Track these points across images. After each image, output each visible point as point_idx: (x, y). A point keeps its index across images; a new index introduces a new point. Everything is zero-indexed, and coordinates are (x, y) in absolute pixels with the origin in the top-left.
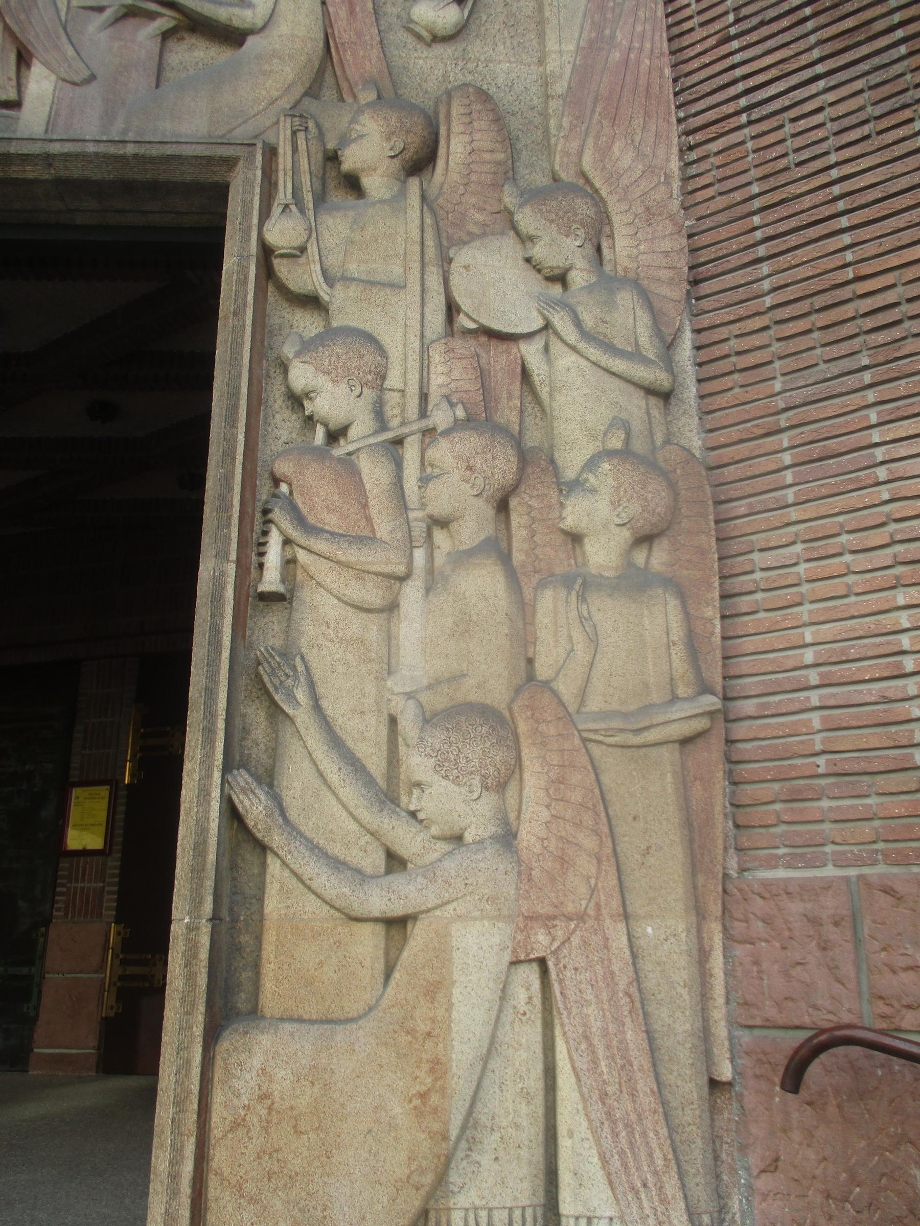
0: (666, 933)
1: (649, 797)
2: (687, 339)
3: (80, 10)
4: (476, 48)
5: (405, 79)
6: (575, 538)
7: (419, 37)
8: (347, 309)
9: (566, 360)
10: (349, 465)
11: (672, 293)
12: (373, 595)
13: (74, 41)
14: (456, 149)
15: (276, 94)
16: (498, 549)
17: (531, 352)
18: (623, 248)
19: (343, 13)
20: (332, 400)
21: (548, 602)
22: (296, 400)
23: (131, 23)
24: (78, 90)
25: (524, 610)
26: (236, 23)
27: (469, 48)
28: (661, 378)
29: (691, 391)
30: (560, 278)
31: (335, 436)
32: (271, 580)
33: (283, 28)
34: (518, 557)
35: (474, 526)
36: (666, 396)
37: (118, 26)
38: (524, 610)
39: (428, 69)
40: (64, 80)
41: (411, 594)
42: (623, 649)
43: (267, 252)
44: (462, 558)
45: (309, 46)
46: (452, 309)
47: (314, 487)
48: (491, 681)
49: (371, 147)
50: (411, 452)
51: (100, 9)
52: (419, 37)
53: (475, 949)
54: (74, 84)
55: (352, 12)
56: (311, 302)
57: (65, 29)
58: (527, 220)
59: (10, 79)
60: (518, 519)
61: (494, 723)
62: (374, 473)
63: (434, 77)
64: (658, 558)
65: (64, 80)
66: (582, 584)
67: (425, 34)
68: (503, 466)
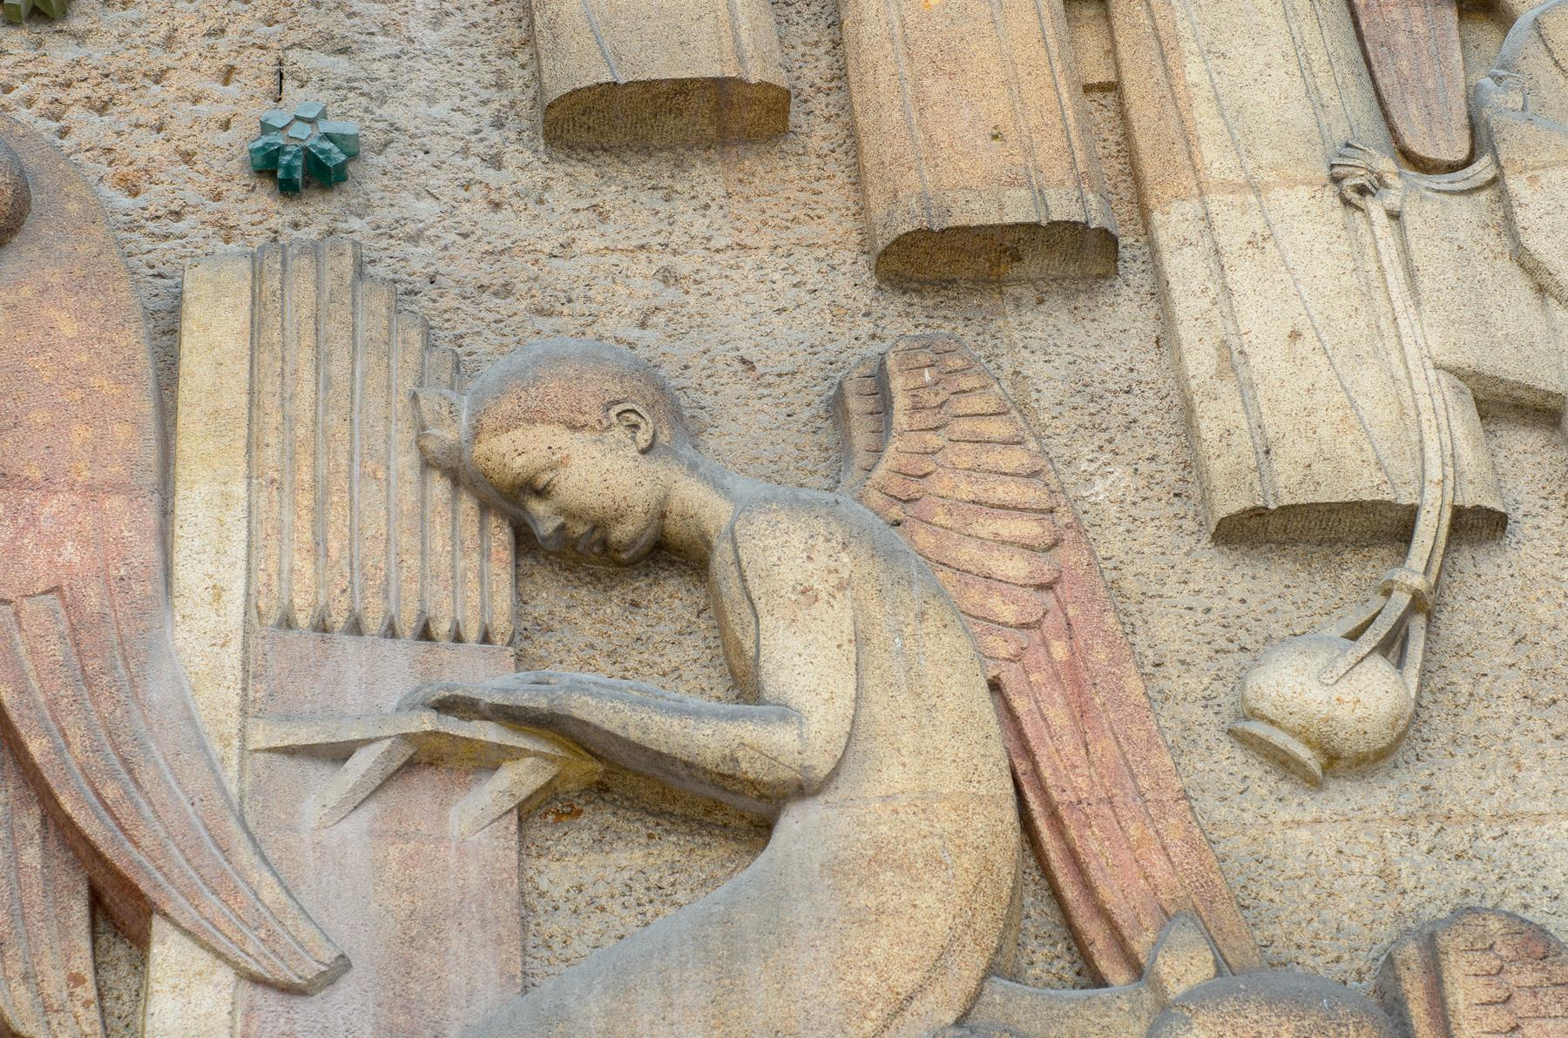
3: (280, 762)
4: (1460, 781)
5: (1267, 892)
7: (1283, 763)
13: (273, 856)
15: (907, 981)
19: (1058, 715)
23: (424, 787)
24: (303, 1008)
26: (751, 768)
27: (1440, 783)
33: (896, 775)
37: (392, 795)
40: (257, 980)
45: (978, 821)
51: (338, 754)
52: (1283, 763)
54: (288, 990)
55: (1082, 712)
57: (241, 820)
59: (77, 980)
63: (1354, 882)
65: (257, 980)
67: (1303, 753)
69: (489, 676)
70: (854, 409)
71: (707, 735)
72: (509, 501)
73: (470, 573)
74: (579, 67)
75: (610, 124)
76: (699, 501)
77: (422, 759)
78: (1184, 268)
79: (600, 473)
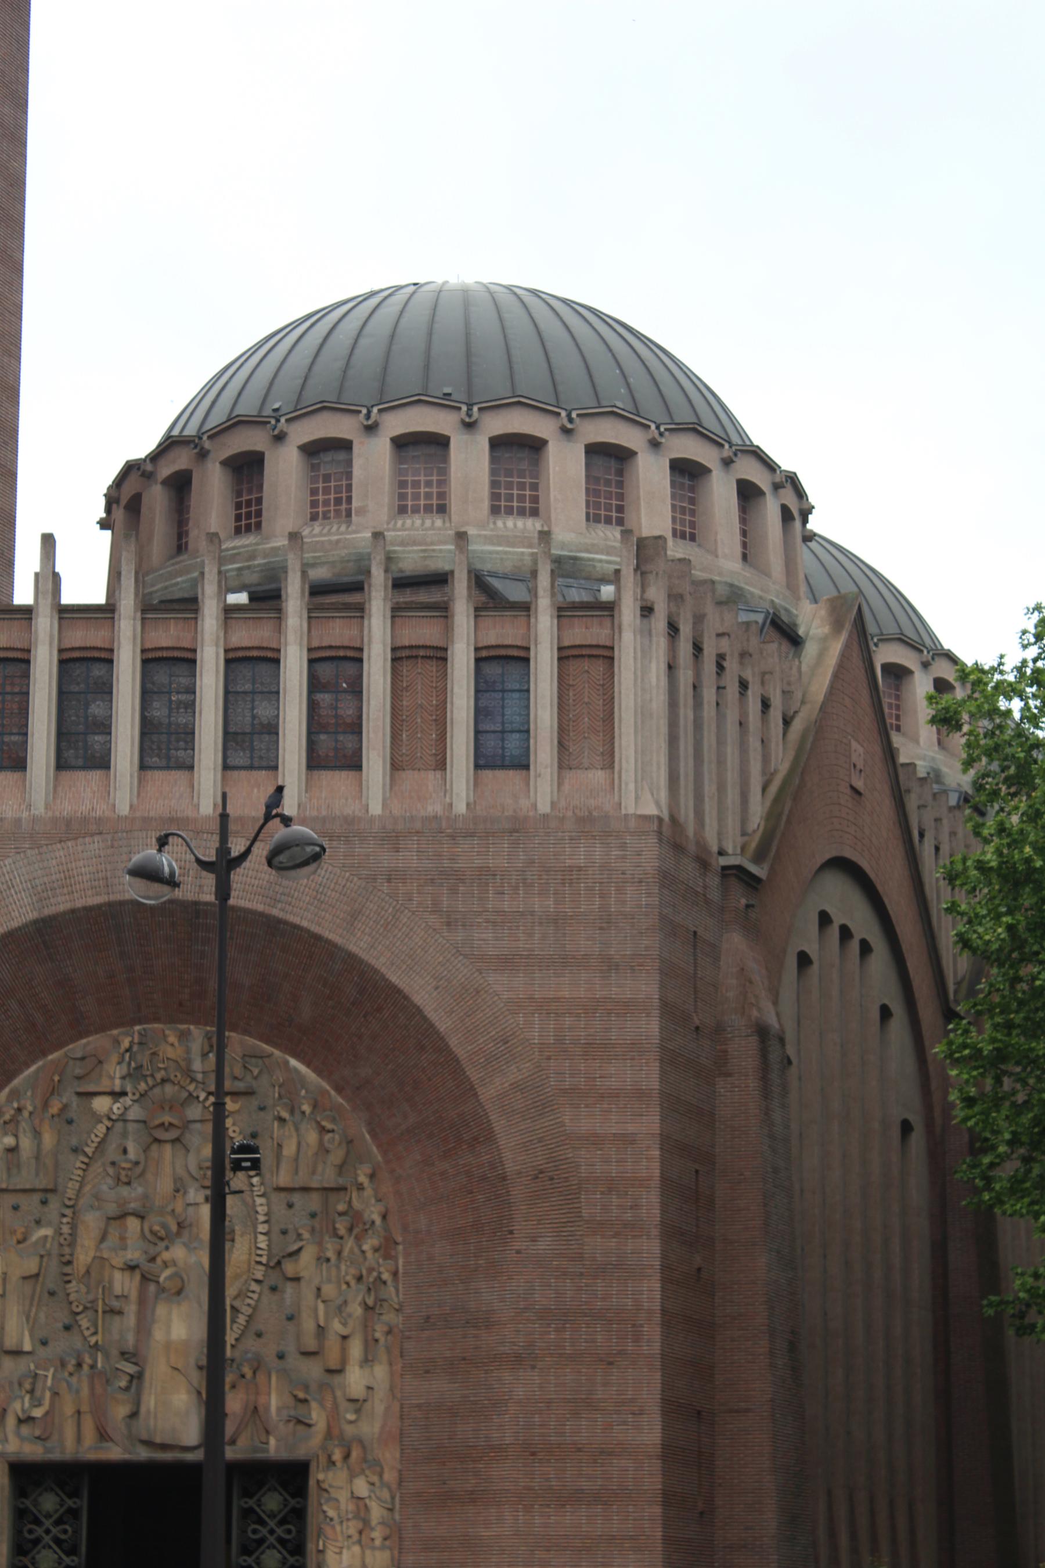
2: (398, 1495)
6: (373, 1539)
8: (334, 1493)
9: (374, 1503)
10: (333, 1527)
11: (394, 1486)
12: (337, 1550)
14: (354, 1454)
16: (359, 1542)
17: (367, 1501)
18: (387, 1476)
20: (331, 1513)
21: (368, 1552)
22: (324, 1512)
25: (363, 1552)
28: (390, 1506)
29: (397, 1506)
30: (373, 1484)
31: (331, 1519)
32: (321, 1547)
34: (363, 1543)
35: (356, 1537)
36: (391, 1510)
38: (363, 1552)
39: (349, 1430)
41: (345, 1551)
43: (318, 1481)
44: (354, 1543)
46: (352, 1493)
47: (328, 1531)
49: (337, 1456)
50: (345, 1524)
56: (326, 1490)
58: (367, 1472)
60: (363, 1536)
62: (338, 1528)
64: (387, 1543)
66: (374, 1548)
68: (360, 1525)
69: (293, 1413)
70: (323, 1386)
71: (307, 1421)
72: (295, 1396)
73: (291, 1402)
74: (302, 1350)
75: (306, 1354)
76: (309, 1398)
77: (289, 1421)
78: (347, 1373)
79: (301, 1395)
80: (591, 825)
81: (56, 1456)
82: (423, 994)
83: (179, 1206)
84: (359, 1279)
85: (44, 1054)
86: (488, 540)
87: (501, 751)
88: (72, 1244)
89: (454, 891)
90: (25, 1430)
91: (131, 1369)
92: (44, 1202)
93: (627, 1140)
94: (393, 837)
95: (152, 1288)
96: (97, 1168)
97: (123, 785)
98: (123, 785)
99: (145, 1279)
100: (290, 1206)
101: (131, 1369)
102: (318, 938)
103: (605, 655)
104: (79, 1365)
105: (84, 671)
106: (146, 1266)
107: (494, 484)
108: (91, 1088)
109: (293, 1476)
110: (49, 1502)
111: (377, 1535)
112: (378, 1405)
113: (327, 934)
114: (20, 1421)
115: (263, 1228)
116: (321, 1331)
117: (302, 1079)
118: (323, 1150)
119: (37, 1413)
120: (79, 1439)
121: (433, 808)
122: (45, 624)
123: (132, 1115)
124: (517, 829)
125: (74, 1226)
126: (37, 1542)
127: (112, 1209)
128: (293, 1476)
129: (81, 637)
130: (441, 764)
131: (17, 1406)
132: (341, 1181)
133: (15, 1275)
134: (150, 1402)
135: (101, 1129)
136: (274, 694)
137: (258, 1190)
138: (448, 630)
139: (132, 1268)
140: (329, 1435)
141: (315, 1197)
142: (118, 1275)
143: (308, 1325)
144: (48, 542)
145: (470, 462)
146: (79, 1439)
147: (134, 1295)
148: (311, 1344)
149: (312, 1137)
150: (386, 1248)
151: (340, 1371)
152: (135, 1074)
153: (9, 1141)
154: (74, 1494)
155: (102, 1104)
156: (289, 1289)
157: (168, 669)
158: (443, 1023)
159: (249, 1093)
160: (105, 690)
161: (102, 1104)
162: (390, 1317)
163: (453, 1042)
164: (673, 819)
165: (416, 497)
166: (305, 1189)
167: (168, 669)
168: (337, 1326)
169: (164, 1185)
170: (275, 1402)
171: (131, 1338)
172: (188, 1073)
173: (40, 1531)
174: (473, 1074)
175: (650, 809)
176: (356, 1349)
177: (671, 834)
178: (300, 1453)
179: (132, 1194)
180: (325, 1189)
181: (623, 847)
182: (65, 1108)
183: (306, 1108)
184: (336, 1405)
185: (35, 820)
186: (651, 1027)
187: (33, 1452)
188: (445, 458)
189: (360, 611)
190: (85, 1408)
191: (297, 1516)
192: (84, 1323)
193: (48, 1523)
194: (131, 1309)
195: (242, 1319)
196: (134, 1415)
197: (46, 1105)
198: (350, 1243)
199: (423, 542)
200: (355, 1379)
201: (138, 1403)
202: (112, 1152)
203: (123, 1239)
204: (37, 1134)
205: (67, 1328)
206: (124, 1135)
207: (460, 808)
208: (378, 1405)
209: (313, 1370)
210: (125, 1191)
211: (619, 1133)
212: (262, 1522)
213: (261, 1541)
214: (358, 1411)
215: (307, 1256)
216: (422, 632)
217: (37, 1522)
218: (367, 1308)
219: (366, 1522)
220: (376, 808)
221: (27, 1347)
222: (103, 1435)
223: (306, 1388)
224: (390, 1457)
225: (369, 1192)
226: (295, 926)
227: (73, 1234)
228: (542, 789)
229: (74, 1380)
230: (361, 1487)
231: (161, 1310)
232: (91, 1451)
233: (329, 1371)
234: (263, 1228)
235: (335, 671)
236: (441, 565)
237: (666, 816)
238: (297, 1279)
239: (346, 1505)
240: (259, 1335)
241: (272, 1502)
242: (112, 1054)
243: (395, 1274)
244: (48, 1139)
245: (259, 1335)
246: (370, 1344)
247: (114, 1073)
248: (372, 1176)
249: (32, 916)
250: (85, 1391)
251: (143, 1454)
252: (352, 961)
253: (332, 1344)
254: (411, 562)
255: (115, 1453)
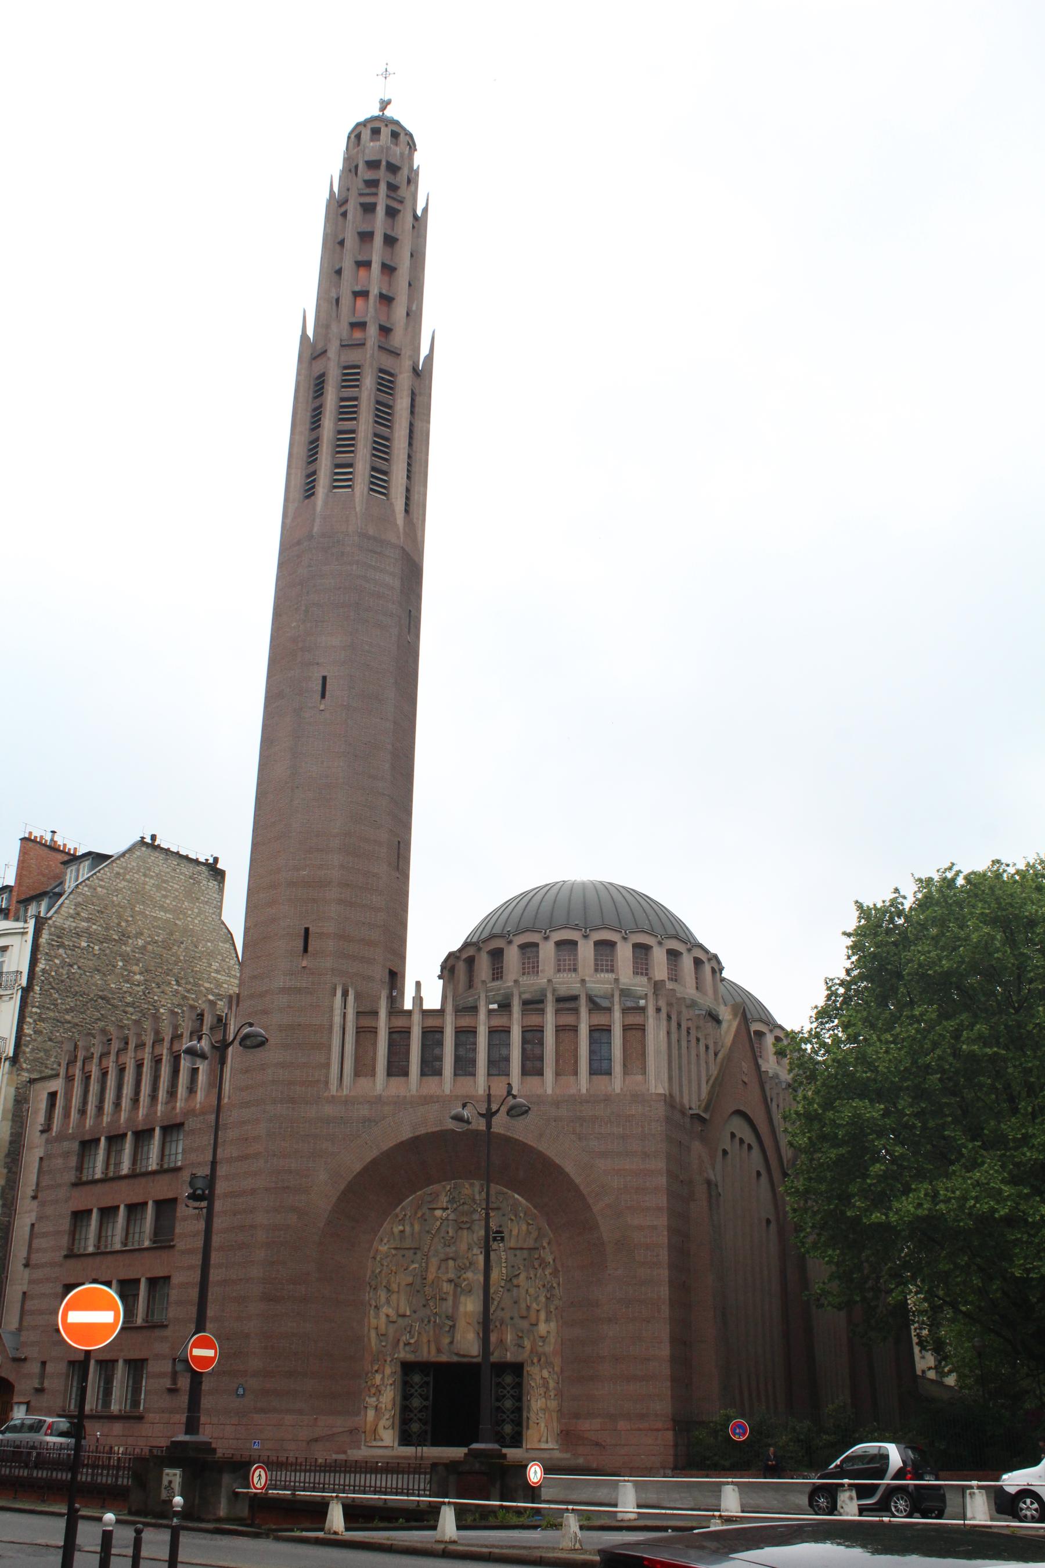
0: (555, 1424)
1: (554, 1415)
39: (540, 1349)
42: (553, 1404)
48: (544, 1406)
49: (535, 1360)
53: (543, 1425)
61: (545, 1410)
75: (522, 1317)
80: (637, 1098)
81: (419, 1359)
82: (569, 1168)
83: (470, 1255)
84: (544, 1286)
85: (415, 1192)
86: (595, 982)
87: (600, 1068)
88: (426, 1271)
89: (582, 1125)
90: (407, 1348)
91: (451, 1323)
92: (415, 1254)
93: (654, 1228)
94: (557, 1104)
95: (459, 1289)
96: (436, 1240)
97: (448, 1081)
98: (448, 1081)
99: (456, 1285)
100: (515, 1255)
101: (451, 1323)
102: (525, 1144)
103: (642, 1028)
104: (429, 1321)
105: (432, 1036)
106: (456, 1280)
107: (596, 960)
108: (434, 1206)
109: (517, 1369)
110: (417, 1378)
111: (552, 1394)
112: (552, 1339)
113: (530, 1143)
114: (405, 1344)
115: (504, 1265)
116: (528, 1307)
117: (520, 1202)
118: (529, 1233)
119: (412, 1341)
120: (429, 1352)
121: (573, 1091)
122: (416, 1018)
123: (451, 1217)
124: (607, 1099)
125: (427, 1263)
126: (412, 1395)
127: (442, 1256)
128: (517, 1369)
129: (431, 1022)
130: (576, 1073)
131: (404, 1338)
132: (537, 1245)
133: (403, 1283)
134: (458, 1337)
135: (438, 1223)
136: (508, 1045)
137: (502, 1249)
138: (578, 1018)
139: (450, 1281)
140: (532, 1352)
141: (525, 1252)
142: (445, 1284)
143: (523, 1306)
144: (418, 984)
145: (586, 951)
146: (429, 1352)
147: (451, 1293)
148: (524, 1314)
149: (524, 1227)
150: (555, 1273)
151: (536, 1325)
152: (452, 1201)
153: (401, 1228)
154: (427, 1375)
155: (438, 1213)
156: (515, 1290)
157: (465, 1035)
158: (578, 1180)
159: (498, 1209)
160: (440, 1043)
161: (438, 1213)
162: (556, 1302)
163: (582, 1188)
164: (671, 1095)
165: (565, 965)
166: (521, 1249)
167: (465, 1035)
168: (534, 1306)
169: (464, 1246)
170: (509, 1338)
171: (450, 1310)
172: (474, 1200)
173: (413, 1391)
174: (591, 1201)
175: (661, 1091)
176: (543, 1316)
177: (670, 1101)
178: (520, 1359)
179: (450, 1250)
180: (530, 1249)
181: (650, 1106)
182: (423, 1214)
183: (522, 1215)
184: (534, 1340)
185: (412, 1096)
186: (663, 1180)
187: (411, 1358)
188: (576, 950)
189: (542, 1011)
190: (432, 1339)
191: (519, 1385)
192: (431, 1304)
193: (417, 1387)
194: (450, 1299)
195: (496, 1303)
196: (452, 1342)
197: (416, 1213)
198: (540, 1271)
199: (567, 983)
200: (543, 1328)
201: (453, 1338)
202: (442, 1234)
203: (447, 1268)
204: (412, 1225)
205: (424, 1306)
206: (448, 1226)
207: (584, 1091)
208: (552, 1339)
209: (525, 1324)
210: (448, 1249)
211: (650, 1225)
212: (504, 1388)
213: (504, 1396)
214: (544, 1341)
215: (522, 1276)
216: (567, 1019)
217: (412, 1387)
218: (547, 1298)
219: (547, 1388)
220: (549, 1091)
221: (408, 1313)
222: (439, 1351)
223: (522, 1331)
224: (557, 1361)
225: (548, 1250)
226: (516, 1140)
227: (427, 1267)
228: (617, 1083)
229: (427, 1328)
230: (545, 1373)
231: (463, 1299)
232: (434, 1357)
233: (532, 1325)
234: (504, 1265)
235: (533, 1036)
236: (575, 992)
237: (667, 1093)
238: (518, 1286)
239: (540, 1381)
240: (503, 1309)
241: (508, 1379)
242: (443, 1192)
243: (559, 1284)
244: (417, 1228)
245: (503, 1309)
246: (549, 1313)
247: (444, 1200)
248: (549, 1243)
249: (411, 1135)
250: (431, 1333)
251: (455, 1359)
252: (540, 1154)
253: (533, 1314)
254: (563, 991)
255: (444, 1358)
